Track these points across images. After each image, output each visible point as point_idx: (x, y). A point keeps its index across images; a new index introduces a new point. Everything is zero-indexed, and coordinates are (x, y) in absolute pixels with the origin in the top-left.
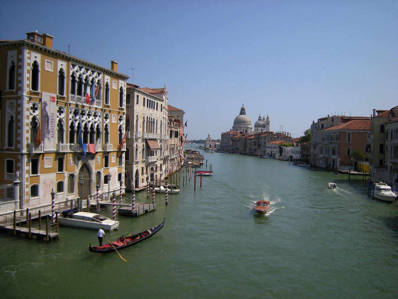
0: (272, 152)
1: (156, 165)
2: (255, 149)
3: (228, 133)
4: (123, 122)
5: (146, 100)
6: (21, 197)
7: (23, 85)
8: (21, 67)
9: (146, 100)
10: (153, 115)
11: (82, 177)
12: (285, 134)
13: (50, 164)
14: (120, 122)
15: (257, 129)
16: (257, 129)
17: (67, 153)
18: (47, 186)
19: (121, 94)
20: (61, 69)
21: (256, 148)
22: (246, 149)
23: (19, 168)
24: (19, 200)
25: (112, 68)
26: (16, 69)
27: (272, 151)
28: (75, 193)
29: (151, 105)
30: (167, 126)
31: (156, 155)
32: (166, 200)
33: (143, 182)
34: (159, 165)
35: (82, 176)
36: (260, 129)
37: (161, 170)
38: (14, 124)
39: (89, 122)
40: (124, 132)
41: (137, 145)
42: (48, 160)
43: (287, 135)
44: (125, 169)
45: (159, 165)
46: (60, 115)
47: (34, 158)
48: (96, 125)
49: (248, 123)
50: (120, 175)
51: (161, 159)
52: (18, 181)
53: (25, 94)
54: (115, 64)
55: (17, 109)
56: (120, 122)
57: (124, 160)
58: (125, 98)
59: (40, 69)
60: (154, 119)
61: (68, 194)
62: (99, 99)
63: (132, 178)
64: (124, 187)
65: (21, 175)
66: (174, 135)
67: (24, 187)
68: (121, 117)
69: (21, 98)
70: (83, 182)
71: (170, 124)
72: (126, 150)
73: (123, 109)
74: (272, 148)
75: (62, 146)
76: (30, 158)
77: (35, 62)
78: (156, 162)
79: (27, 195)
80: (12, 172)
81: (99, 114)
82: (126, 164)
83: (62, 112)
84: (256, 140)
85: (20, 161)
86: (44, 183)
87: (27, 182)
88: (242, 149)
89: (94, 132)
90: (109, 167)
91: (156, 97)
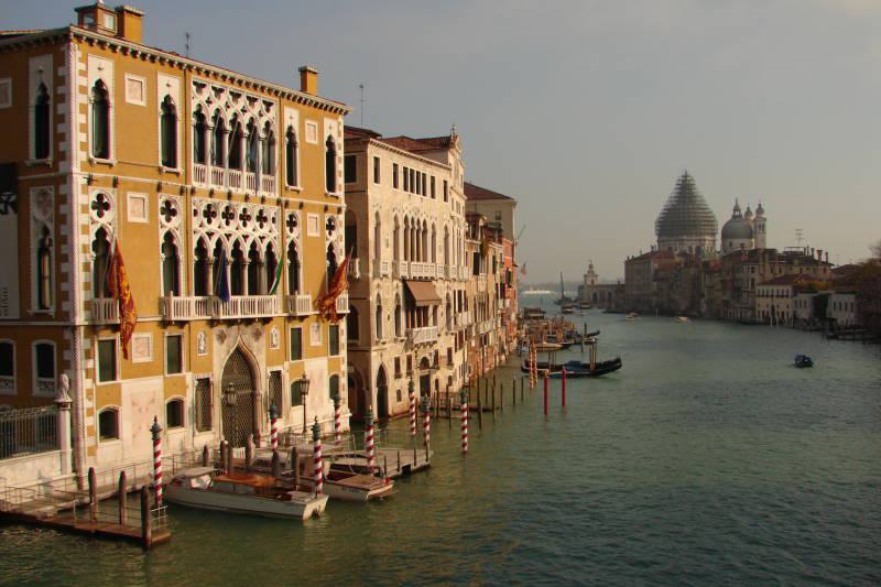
0: (773, 308)
1: (437, 352)
4: (341, 231)
5: (401, 170)
6: (75, 441)
7: (70, 145)
8: (64, 98)
9: (401, 170)
10: (422, 211)
11: (230, 386)
13: (146, 353)
14: (330, 234)
15: (731, 244)
18: (140, 410)
19: (331, 156)
20: (168, 98)
23: (68, 365)
25: (304, 88)
26: (51, 103)
27: (775, 305)
28: (213, 430)
29: (414, 183)
31: (435, 323)
32: (464, 445)
33: (399, 399)
34: (443, 353)
36: (737, 242)
37: (450, 363)
38: (52, 249)
39: (246, 237)
40: (340, 259)
41: (378, 295)
42: (141, 341)
43: (816, 257)
44: (350, 364)
45: (443, 353)
46: (168, 220)
48: (262, 248)
50: (334, 381)
53: (76, 169)
54: (309, 75)
55: (57, 209)
56: (330, 234)
57: (343, 339)
58: (340, 167)
59: (112, 101)
61: (197, 433)
62: (269, 173)
63: (369, 388)
64: (345, 415)
65: (73, 383)
68: (330, 220)
69: (66, 178)
70: (233, 399)
71: (472, 235)
72: (349, 312)
73: (337, 197)
74: (775, 298)
75: (177, 304)
77: (99, 83)
78: (435, 342)
79: (89, 435)
81: (272, 215)
82: (351, 349)
83: (174, 213)
84: (728, 274)
85: (68, 345)
86: (134, 404)
87: (90, 399)
89: (260, 264)
91: (428, 162)
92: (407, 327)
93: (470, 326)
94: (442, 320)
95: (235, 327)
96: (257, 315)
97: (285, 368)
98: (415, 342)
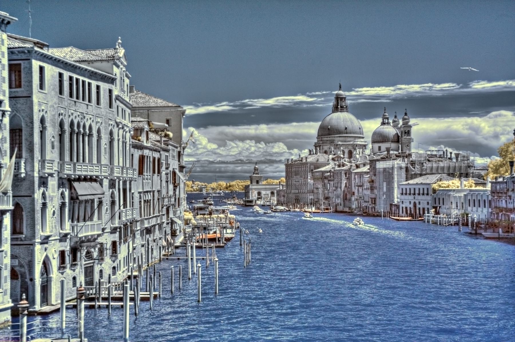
0: (415, 203)
2: (372, 198)
3: (301, 161)
10: (87, 117)
12: (449, 156)
15: (380, 148)
16: (380, 148)
21: (373, 196)
22: (350, 200)
27: (417, 202)
30: (128, 145)
44: (13, 257)
49: (354, 133)
51: (114, 231)
60: (90, 128)
63: (32, 280)
66: (148, 165)
74: (417, 196)
78: (99, 235)
88: (339, 201)
93: (137, 221)
98: (80, 235)
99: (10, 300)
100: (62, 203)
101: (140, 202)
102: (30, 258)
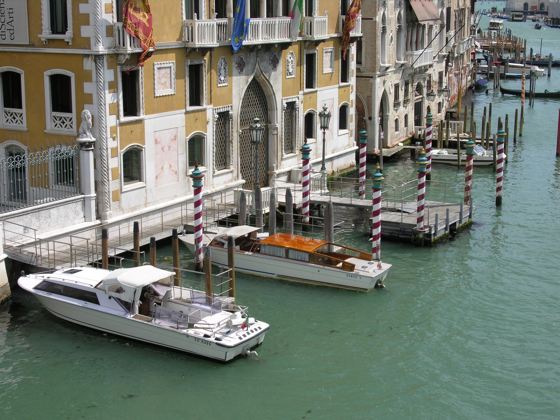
1: (430, 76)
11: (257, 122)
13: (168, 84)
17: (211, 49)
18: (163, 149)
24: (93, 194)
32: (499, 189)
35: (257, 119)
41: (384, 14)
42: (163, 71)
45: (435, 78)
47: (127, 68)
50: (343, 110)
52: (89, 138)
61: (217, 172)
67: (107, 156)
76: (119, 67)
78: (431, 66)
80: (68, 109)
86: (156, 142)
90: (316, 89)
92: (407, 50)
94: (436, 42)
95: (254, 54)
96: (277, 40)
97: (299, 99)
98: (415, 67)
99: (355, 142)
100: (399, 26)
101: (455, 22)
102: (369, 93)
